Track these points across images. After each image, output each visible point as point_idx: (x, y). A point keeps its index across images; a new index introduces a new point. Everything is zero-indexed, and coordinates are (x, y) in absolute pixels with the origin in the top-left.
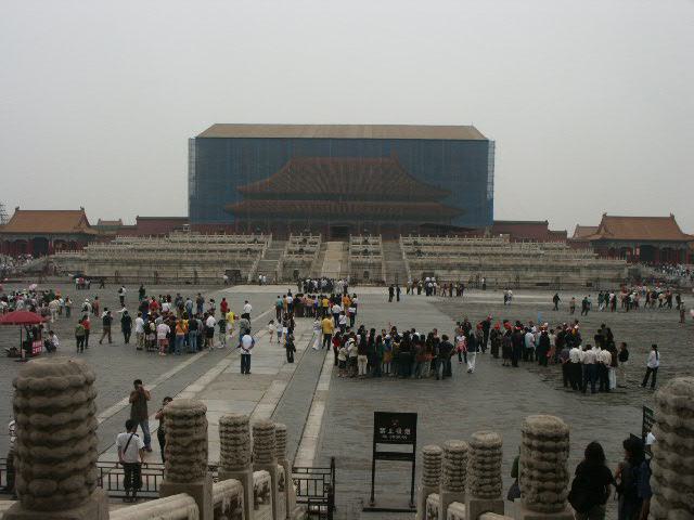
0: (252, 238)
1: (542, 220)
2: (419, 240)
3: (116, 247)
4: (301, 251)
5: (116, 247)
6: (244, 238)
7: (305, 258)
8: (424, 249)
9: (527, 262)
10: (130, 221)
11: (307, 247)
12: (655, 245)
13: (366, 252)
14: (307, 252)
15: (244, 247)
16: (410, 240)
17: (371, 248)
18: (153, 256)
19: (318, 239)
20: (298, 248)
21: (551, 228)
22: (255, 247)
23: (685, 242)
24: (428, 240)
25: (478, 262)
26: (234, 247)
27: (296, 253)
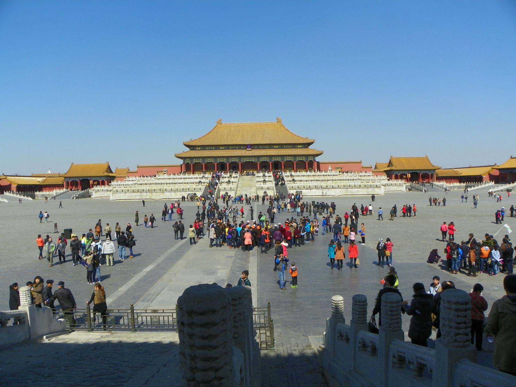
0: (202, 175)
1: (359, 161)
2: (293, 173)
3: (127, 183)
4: (229, 181)
5: (127, 183)
6: (196, 175)
7: (231, 185)
8: (296, 178)
9: (352, 183)
10: (135, 169)
11: (232, 180)
12: (418, 172)
13: (264, 181)
14: (232, 182)
15: (198, 180)
16: (288, 174)
18: (148, 187)
19: (238, 175)
21: (364, 164)
22: (203, 180)
23: (434, 170)
24: (298, 173)
25: (325, 184)
27: (227, 182)
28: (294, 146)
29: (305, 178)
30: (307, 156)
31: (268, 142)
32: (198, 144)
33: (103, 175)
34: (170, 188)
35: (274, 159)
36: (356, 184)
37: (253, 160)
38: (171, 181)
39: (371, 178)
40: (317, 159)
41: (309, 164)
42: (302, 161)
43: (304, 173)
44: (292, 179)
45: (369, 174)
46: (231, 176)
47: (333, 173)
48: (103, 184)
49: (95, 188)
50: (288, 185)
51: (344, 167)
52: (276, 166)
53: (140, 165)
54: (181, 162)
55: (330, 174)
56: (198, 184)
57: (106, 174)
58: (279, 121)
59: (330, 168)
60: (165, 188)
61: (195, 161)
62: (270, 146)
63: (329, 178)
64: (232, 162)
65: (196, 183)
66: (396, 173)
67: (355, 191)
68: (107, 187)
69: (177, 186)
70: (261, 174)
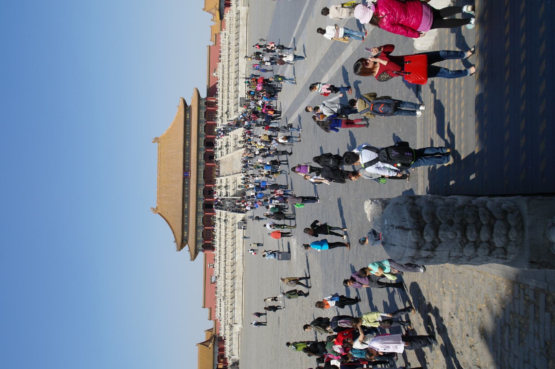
0: (217, 222)
2: (219, 116)
3: (222, 317)
5: (222, 317)
6: (217, 228)
7: (230, 184)
8: (225, 110)
10: (207, 310)
15: (223, 224)
16: (219, 122)
17: (224, 144)
19: (218, 179)
20: (224, 191)
21: (212, 44)
22: (223, 218)
24: (219, 111)
26: (223, 231)
28: (187, 123)
29: (225, 101)
30: (199, 108)
31: (181, 153)
32: (180, 233)
33: (212, 349)
34: (231, 254)
35: (202, 146)
36: (234, 39)
37: (202, 170)
38: (223, 257)
39: (227, 32)
40: (204, 95)
41: (208, 106)
42: (205, 113)
43: (219, 104)
44: (226, 116)
45: (224, 34)
46: (219, 187)
47: (220, 70)
48: (222, 349)
49: (227, 354)
50: (233, 117)
51: (214, 55)
52: (210, 144)
53: (202, 304)
54: (201, 255)
55: (221, 74)
56: (227, 223)
57: (211, 345)
58: (157, 140)
59: (214, 74)
60: (230, 261)
61: (200, 238)
62: (186, 150)
63: (226, 72)
64: (203, 194)
65: (225, 223)
66: (223, 5)
67: (242, 41)
68: (227, 342)
69: (230, 249)
70: (218, 153)
